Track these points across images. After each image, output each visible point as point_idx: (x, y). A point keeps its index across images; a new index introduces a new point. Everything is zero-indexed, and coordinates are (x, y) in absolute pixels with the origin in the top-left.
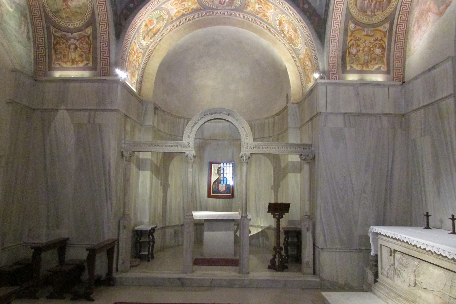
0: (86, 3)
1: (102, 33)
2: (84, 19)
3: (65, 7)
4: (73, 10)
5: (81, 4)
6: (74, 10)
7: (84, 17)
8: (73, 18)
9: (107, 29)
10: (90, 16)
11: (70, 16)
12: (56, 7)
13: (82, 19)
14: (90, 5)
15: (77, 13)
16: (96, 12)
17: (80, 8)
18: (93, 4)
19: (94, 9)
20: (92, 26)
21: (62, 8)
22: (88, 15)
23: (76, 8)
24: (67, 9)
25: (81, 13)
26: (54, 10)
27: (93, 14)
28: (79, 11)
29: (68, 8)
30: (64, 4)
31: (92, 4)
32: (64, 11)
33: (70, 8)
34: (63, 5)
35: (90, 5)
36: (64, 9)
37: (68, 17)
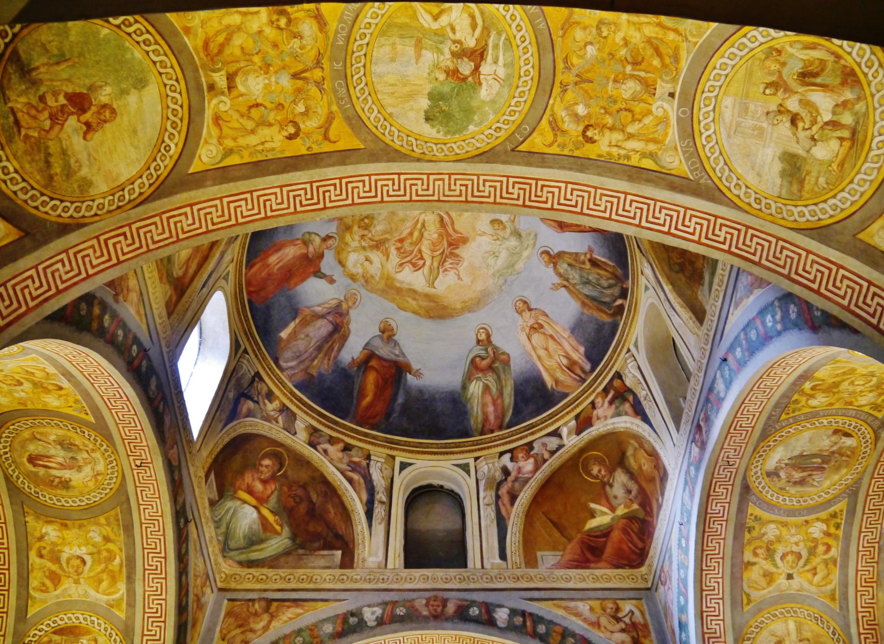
0: (92, 192)
1: (11, 292)
2: (33, 198)
3: (51, 101)
4: (50, 143)
5: (84, 172)
6: (53, 147)
7: (42, 194)
8: (20, 145)
9: (31, 304)
10: (53, 217)
11: (23, 132)
12: (39, 60)
13: (33, 188)
14: (89, 208)
15: (48, 164)
16: (72, 238)
17: (69, 173)
18: (97, 218)
19: (80, 226)
20: (20, 238)
21: (43, 89)
22: (54, 208)
23: (64, 152)
24: (46, 114)
25: (51, 178)
26: (22, 48)
27: (64, 229)
28: (57, 169)
29: (53, 117)
30: (62, 100)
31: (96, 215)
32: (34, 101)
33: (57, 128)
34: (55, 94)
35: (89, 208)
36: (42, 99)
37: (17, 122)
